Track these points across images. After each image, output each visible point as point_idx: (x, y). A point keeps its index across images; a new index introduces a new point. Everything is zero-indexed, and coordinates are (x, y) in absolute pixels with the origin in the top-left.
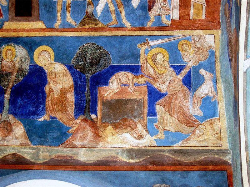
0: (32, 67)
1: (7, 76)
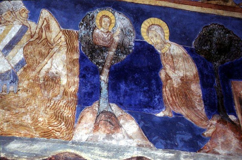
0: (138, 44)
1: (102, 51)
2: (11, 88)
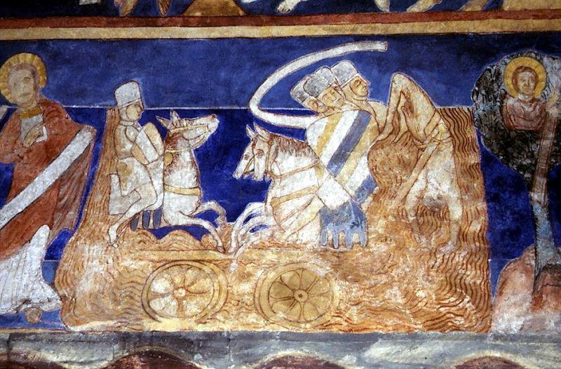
2: (355, 237)
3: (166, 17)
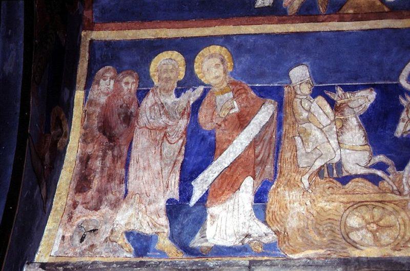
3: (326, 15)
